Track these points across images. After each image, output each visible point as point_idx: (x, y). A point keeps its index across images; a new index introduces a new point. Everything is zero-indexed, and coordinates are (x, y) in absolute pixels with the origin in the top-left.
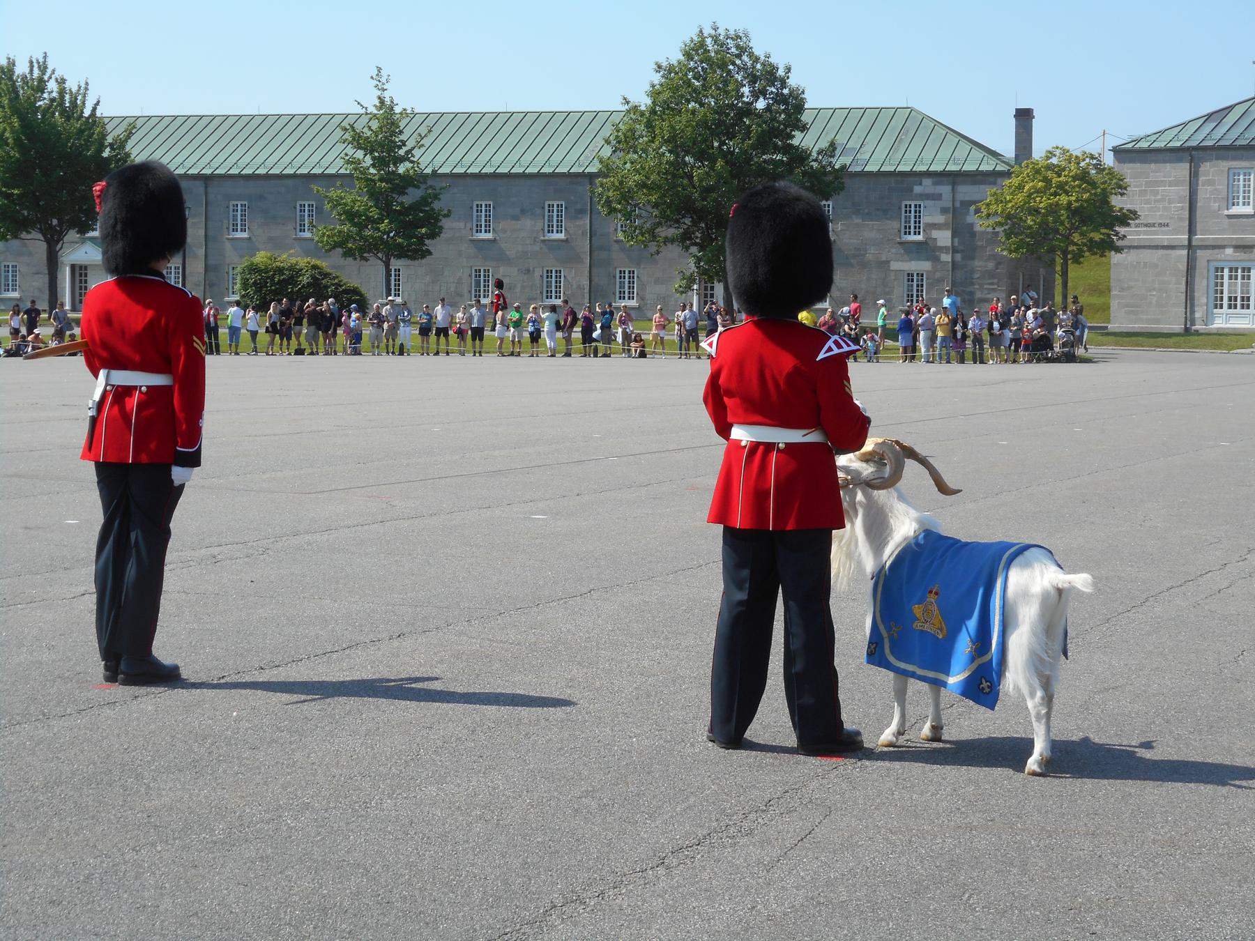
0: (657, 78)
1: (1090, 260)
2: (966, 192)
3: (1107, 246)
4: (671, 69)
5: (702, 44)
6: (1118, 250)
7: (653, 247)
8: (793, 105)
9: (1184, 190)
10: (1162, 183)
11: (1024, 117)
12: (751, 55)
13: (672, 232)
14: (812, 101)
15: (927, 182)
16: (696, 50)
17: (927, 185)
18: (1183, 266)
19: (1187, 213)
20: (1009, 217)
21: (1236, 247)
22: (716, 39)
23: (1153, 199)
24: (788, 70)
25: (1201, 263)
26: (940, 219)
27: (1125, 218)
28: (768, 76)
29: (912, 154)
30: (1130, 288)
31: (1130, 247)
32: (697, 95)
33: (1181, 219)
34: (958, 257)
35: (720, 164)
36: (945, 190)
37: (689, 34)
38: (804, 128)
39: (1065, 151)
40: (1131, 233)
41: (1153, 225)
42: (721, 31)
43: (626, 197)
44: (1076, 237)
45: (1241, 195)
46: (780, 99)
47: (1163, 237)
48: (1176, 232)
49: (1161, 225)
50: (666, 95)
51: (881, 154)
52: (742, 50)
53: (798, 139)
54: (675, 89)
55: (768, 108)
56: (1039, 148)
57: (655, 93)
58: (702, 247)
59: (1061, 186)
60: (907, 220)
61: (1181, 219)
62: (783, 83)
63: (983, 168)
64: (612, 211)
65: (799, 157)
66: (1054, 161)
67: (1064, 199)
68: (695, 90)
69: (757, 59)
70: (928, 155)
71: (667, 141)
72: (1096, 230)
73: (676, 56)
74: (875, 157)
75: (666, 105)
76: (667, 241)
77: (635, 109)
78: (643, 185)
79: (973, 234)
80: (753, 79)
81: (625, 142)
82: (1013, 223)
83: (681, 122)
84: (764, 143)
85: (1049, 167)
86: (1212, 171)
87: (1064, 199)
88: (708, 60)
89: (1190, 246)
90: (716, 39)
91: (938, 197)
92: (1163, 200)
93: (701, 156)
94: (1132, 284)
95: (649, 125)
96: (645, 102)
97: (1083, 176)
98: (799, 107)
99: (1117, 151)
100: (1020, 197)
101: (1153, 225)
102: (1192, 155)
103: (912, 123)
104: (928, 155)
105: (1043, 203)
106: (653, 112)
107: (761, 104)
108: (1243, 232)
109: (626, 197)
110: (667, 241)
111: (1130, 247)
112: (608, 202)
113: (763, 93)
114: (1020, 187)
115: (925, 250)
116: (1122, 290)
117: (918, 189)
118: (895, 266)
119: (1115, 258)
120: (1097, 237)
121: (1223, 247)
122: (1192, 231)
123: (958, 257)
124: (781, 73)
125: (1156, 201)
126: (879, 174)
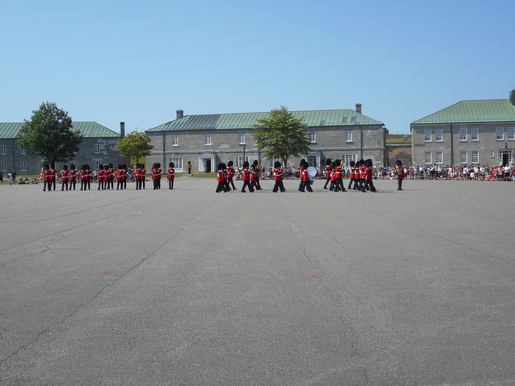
0: (33, 115)
1: (142, 157)
2: (110, 142)
3: (145, 154)
4: (37, 112)
5: (45, 106)
6: (149, 155)
7: (33, 156)
8: (69, 122)
9: (162, 141)
10: (157, 139)
11: (122, 124)
12: (57, 109)
13: (38, 153)
14: (73, 120)
15: (100, 140)
16: (43, 107)
17: (100, 140)
18: (163, 159)
20: (123, 148)
21: (175, 154)
22: (48, 105)
23: (156, 142)
24: (67, 112)
25: (167, 157)
26: (104, 148)
27: (151, 147)
28: (62, 114)
29: (96, 133)
32: (44, 119)
34: (109, 157)
35: (52, 135)
36: (105, 141)
37: (41, 104)
38: (72, 127)
39: (136, 132)
40: (152, 151)
42: (49, 103)
43: (26, 144)
44: (140, 152)
46: (65, 119)
47: (158, 152)
50: (36, 118)
51: (88, 133)
52: (55, 108)
53: (70, 129)
54: (38, 117)
55: (62, 122)
56: (128, 131)
57: (33, 118)
58: (46, 156)
59: (136, 140)
60: (96, 149)
62: (66, 116)
63: (114, 136)
64: (23, 147)
65: (71, 134)
66: (134, 134)
67: (137, 143)
68: (43, 118)
69: (58, 110)
70: (100, 133)
71: (37, 130)
72: (144, 150)
73: (38, 109)
74: (87, 134)
75: (36, 121)
76: (37, 155)
77: (28, 122)
78: (32, 141)
79: (112, 152)
80: (58, 114)
81: (25, 130)
82: (124, 150)
83: (40, 125)
84: (62, 131)
85: (133, 136)
86: (169, 138)
87: (137, 143)
88: (46, 110)
89: (164, 154)
90: (48, 105)
91: (103, 143)
93: (45, 133)
95: (32, 127)
96: (30, 120)
97: (141, 138)
98: (70, 122)
99: (146, 132)
100: (127, 143)
102: (163, 133)
103: (95, 126)
104: (100, 133)
105: (132, 144)
106: (32, 123)
107: (60, 121)
109: (26, 144)
110: (37, 155)
112: (22, 145)
113: (61, 118)
114: (126, 141)
115: (101, 155)
117: (98, 141)
118: (94, 160)
119: (148, 156)
120: (144, 152)
121: (171, 154)
122: (164, 150)
123: (109, 157)
124: (65, 113)
126: (88, 138)
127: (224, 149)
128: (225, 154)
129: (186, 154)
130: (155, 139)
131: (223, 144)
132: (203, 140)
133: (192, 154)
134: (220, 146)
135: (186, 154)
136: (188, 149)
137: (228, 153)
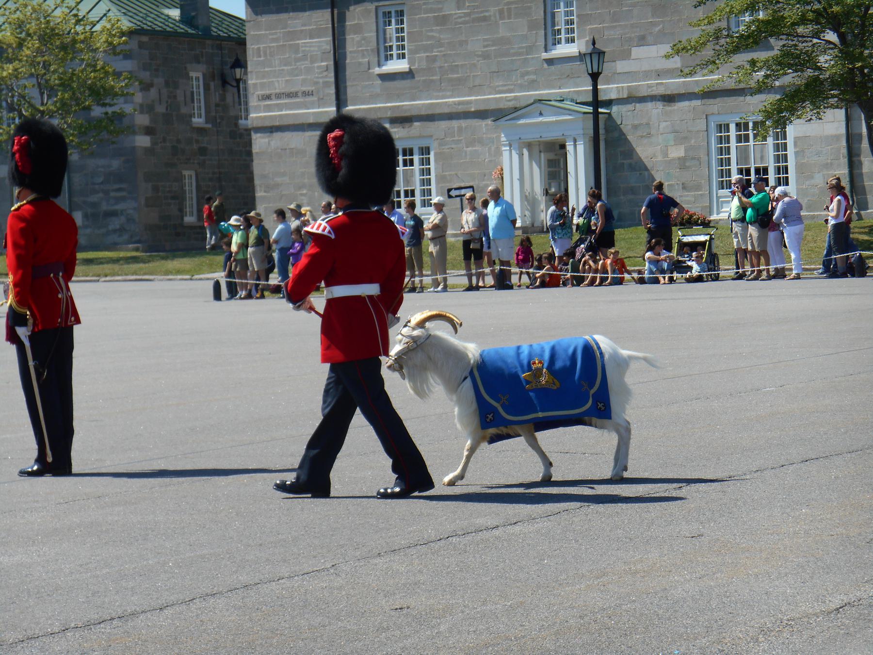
9: (325, 42)
19: (332, 74)
30: (277, 186)
31: (272, 130)
33: (326, 84)
41: (294, 95)
45: (394, 44)
48: (321, 102)
49: (306, 94)
61: (326, 84)
92: (304, 57)
94: (279, 180)
101: (294, 95)
108: (399, 98)
111: (272, 130)
116: (268, 188)
122: (340, 100)
125: (297, 60)
127: (647, 75)
128: (655, 109)
129: (450, 116)
130: (293, 35)
131: (642, 41)
132: (532, 26)
133: (481, 115)
134: (626, 55)
135: (450, 116)
136: (457, 85)
137: (669, 99)
